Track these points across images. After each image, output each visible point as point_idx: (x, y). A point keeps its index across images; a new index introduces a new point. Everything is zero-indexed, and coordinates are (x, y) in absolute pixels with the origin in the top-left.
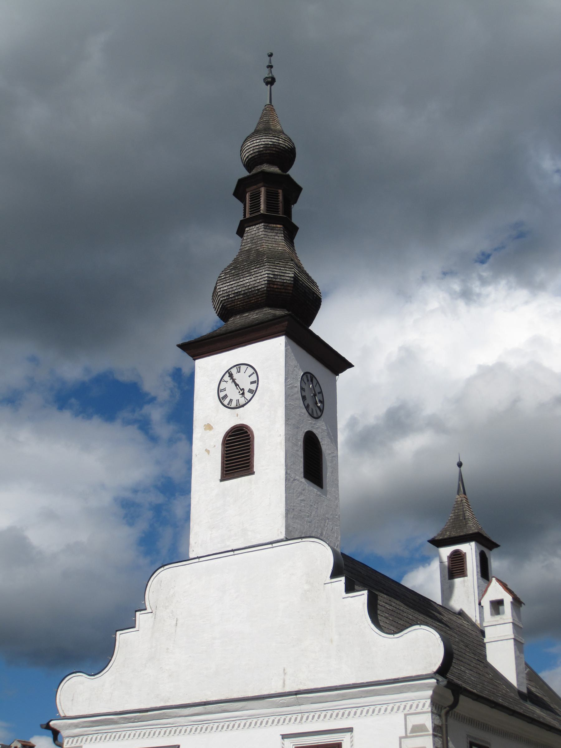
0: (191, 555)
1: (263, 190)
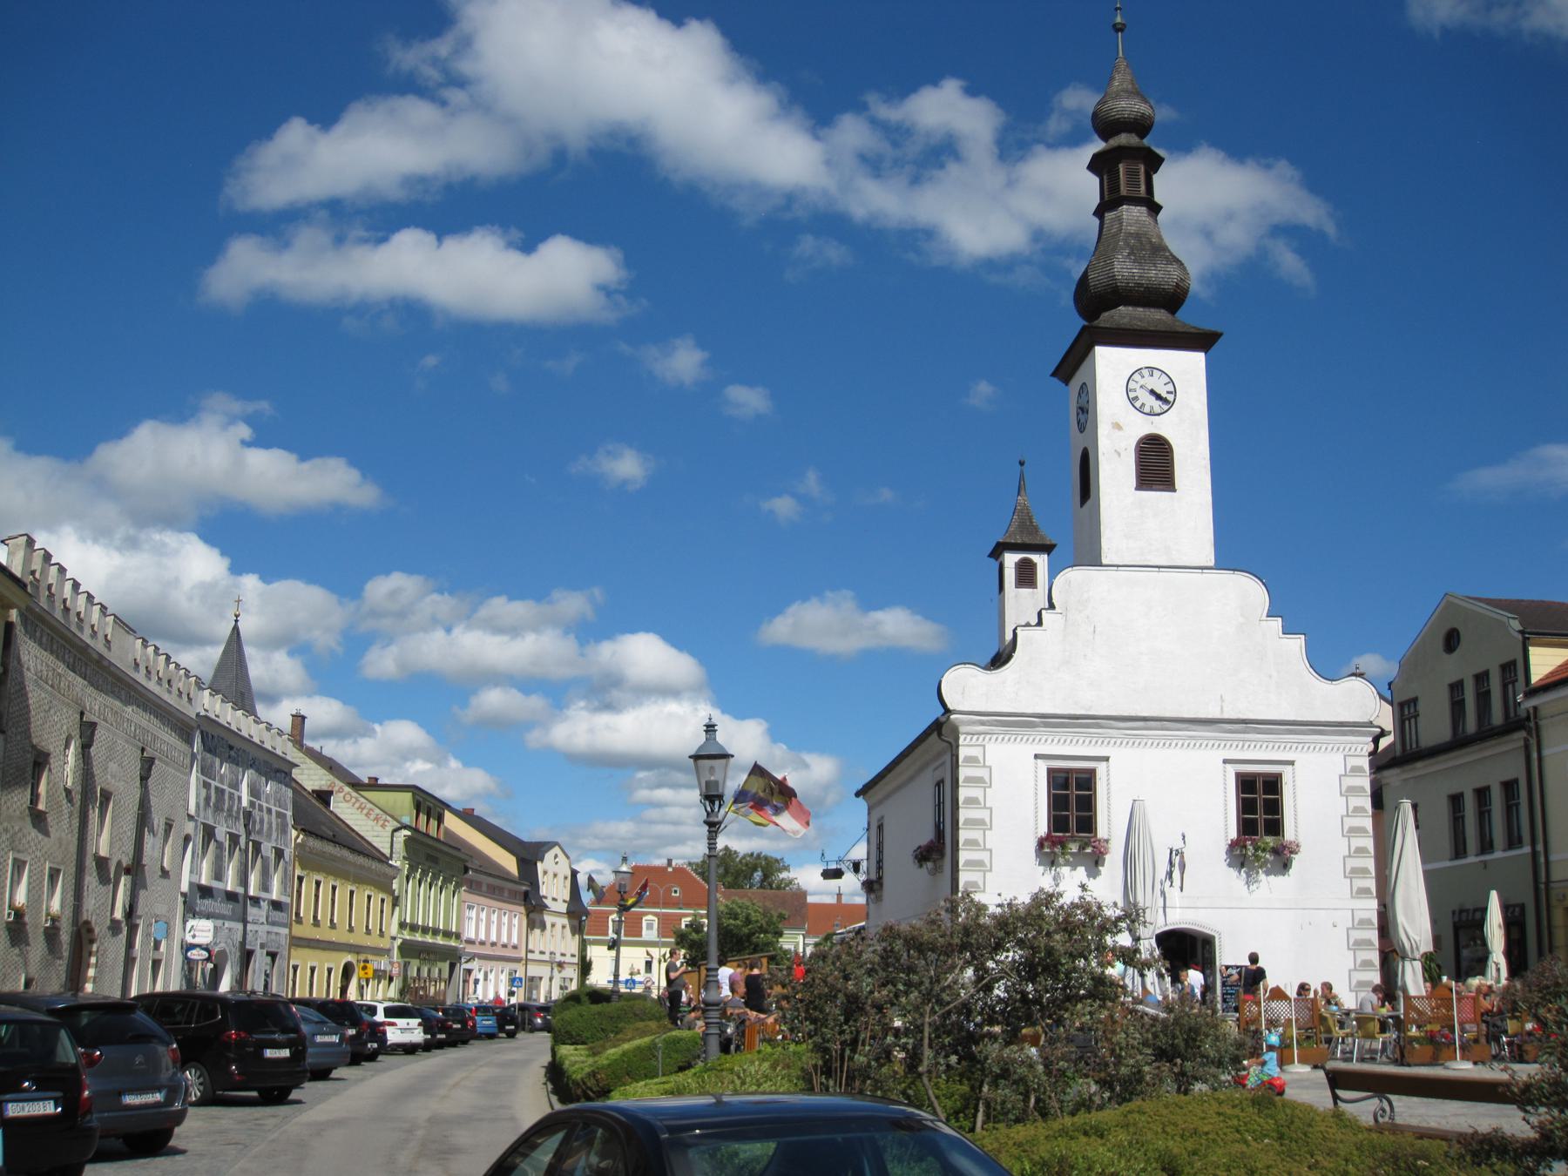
0: (1104, 561)
1: (1142, 168)
